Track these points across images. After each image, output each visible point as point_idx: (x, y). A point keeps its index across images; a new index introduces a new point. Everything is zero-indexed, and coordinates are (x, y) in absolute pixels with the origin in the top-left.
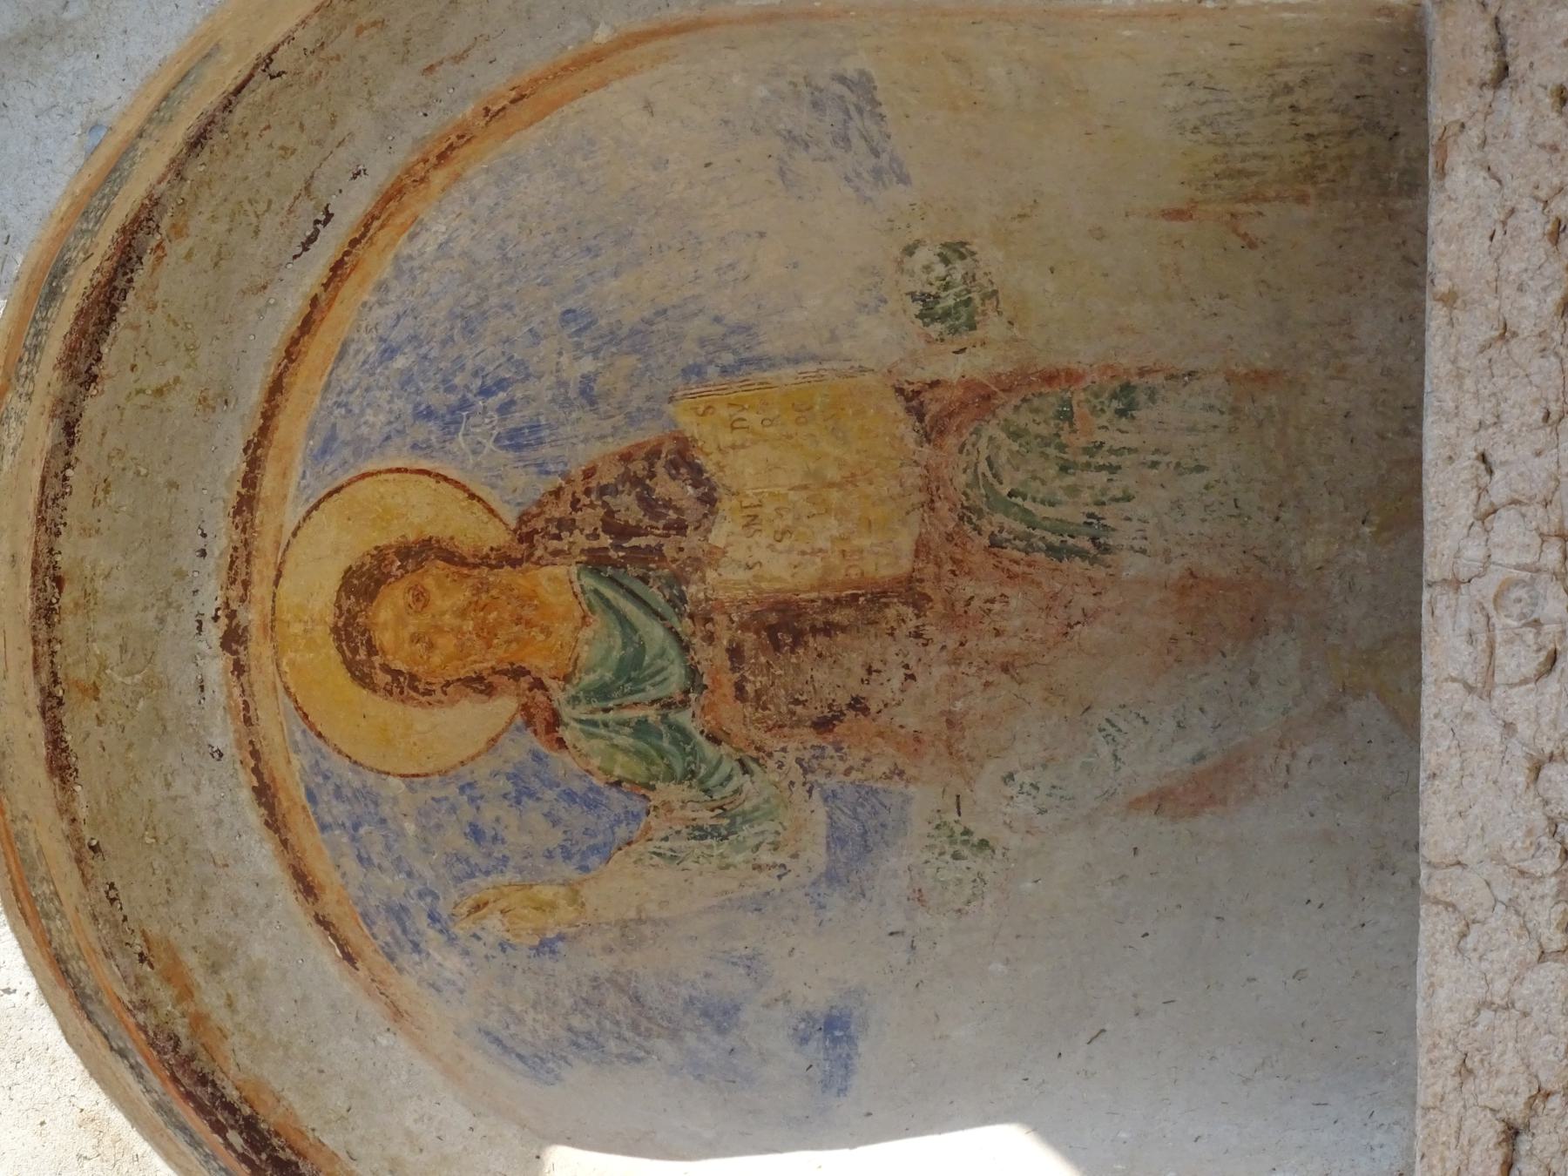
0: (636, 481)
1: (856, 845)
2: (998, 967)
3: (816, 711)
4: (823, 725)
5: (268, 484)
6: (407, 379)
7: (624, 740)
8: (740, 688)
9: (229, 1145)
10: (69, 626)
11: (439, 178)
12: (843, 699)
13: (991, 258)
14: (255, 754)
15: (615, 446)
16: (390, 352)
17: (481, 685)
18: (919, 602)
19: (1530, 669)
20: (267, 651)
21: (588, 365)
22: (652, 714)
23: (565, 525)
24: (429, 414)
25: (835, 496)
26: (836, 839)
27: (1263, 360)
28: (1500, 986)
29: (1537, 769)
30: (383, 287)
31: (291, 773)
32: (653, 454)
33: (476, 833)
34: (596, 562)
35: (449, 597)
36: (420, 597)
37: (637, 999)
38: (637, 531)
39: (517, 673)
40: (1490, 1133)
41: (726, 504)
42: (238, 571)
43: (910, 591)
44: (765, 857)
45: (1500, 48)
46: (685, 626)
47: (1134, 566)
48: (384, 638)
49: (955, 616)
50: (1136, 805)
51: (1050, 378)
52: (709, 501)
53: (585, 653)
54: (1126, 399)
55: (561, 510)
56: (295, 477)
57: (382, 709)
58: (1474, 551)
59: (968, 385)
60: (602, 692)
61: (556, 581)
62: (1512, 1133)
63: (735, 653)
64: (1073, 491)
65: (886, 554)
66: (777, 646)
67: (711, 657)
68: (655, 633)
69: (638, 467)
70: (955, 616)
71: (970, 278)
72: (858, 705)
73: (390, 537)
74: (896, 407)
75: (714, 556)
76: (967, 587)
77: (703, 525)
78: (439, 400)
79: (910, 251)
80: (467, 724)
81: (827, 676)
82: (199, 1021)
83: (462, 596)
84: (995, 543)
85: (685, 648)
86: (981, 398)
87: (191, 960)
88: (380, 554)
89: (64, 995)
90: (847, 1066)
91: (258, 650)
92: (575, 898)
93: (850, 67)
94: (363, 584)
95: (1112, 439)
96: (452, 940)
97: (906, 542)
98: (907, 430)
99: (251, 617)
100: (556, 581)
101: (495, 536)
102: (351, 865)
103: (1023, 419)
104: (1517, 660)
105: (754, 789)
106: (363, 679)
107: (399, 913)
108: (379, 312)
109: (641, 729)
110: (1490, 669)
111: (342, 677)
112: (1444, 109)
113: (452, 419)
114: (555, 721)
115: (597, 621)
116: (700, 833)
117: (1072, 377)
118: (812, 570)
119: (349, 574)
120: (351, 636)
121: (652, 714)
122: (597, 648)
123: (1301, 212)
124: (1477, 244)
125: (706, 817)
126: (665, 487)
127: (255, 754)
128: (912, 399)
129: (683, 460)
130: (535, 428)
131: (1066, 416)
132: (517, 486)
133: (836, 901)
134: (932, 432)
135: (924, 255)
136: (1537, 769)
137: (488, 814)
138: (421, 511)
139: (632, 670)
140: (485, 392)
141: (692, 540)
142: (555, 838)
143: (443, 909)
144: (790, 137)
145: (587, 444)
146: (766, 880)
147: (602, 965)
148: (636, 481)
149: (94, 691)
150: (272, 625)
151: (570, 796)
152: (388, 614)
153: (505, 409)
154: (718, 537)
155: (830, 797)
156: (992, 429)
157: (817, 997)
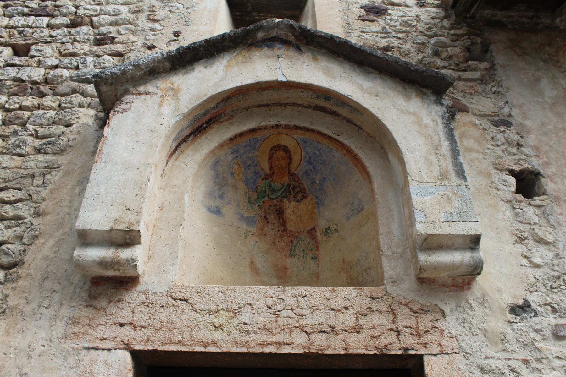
0: (301, 191)
1: (248, 220)
2: (227, 236)
3: (267, 216)
4: (265, 217)
5: (299, 132)
6: (315, 154)
7: (263, 189)
8: (271, 206)
9: (204, 123)
10: (279, 107)
11: (345, 152)
12: (269, 220)
13: (335, 236)
14: (260, 129)
15: (306, 187)
16: (319, 150)
17: (271, 168)
18: (283, 231)
19: (268, 303)
20: (275, 132)
21: (318, 182)
22: (267, 193)
23: (294, 181)
24: (310, 158)
25: (299, 219)
26: (248, 217)
27: (321, 277)
28: (212, 298)
29: (250, 305)
30: (328, 147)
31: (258, 136)
32: (305, 193)
33: (250, 166)
34: (289, 185)
35: (283, 163)
36: (284, 159)
37: (224, 186)
38: (294, 191)
39: (273, 174)
40: (186, 297)
41: (298, 204)
42: (287, 127)
43: (285, 230)
44: (246, 208)
45: (378, 298)
46: (280, 198)
47: (289, 261)
48: (278, 153)
49: (281, 236)
50: (252, 259)
51: (317, 247)
52: (298, 201)
53: (276, 184)
54: (315, 258)
55: (296, 180)
56: (301, 137)
57: (268, 151)
58: (289, 295)
59: (316, 236)
60: (270, 186)
61: (286, 180)
62: (186, 300)
63: (276, 205)
64: (300, 252)
65: (291, 227)
66: (277, 211)
67: (275, 202)
68: (279, 194)
69: (303, 191)
70: (281, 236)
71: (332, 233)
72: (268, 222)
73: (292, 154)
74: (312, 227)
75: (290, 202)
76: (285, 237)
77: (295, 201)
78: (312, 159)
79: (336, 225)
80: (265, 166)
81: (271, 218)
82: (222, 122)
83: (284, 165)
84: (292, 241)
85: (277, 198)
86: (314, 238)
87: (231, 121)
88: (290, 152)
89: (225, 96)
90: (212, 212)
91: (275, 131)
92: (240, 179)
93: (366, 207)
94: (285, 149)
95: (308, 257)
96: (234, 159)
97: (292, 229)
98: (309, 228)
99: (280, 129)
100: (286, 180)
101: (293, 170)
102: (244, 144)
103: (311, 244)
104: (270, 302)
105: (256, 207)
106: (272, 149)
107: (237, 151)
108: (324, 147)
109: (265, 192)
110: (268, 297)
111: (272, 146)
112: (366, 289)
113: (309, 162)
114: (266, 179)
115: (281, 186)
116: (249, 199)
117: (318, 250)
118: (288, 216)
119: (286, 147)
120: (278, 147)
121: (267, 193)
122: (277, 186)
123: (345, 280)
124: (343, 295)
125: (252, 200)
126: (300, 195)
127: (260, 129)
128: (314, 229)
129: (304, 197)
130: (308, 175)
131: (312, 250)
132: (300, 173)
133: (239, 216)
134: (309, 232)
135: (335, 227)
136: (250, 305)
137: (253, 168)
138: (296, 158)
139: (273, 191)
140: (313, 167)
141: (292, 199)
142: (249, 178)
143: (238, 159)
144: (353, 203)
145: (306, 183)
146: (242, 207)
147: (230, 182)
148: (301, 191)
149: (270, 110)
150: (279, 133)
151: (255, 180)
152: (281, 153)
153: (311, 170)
154: (293, 203)
155: (254, 217)
156: (309, 240)
157: (224, 211)
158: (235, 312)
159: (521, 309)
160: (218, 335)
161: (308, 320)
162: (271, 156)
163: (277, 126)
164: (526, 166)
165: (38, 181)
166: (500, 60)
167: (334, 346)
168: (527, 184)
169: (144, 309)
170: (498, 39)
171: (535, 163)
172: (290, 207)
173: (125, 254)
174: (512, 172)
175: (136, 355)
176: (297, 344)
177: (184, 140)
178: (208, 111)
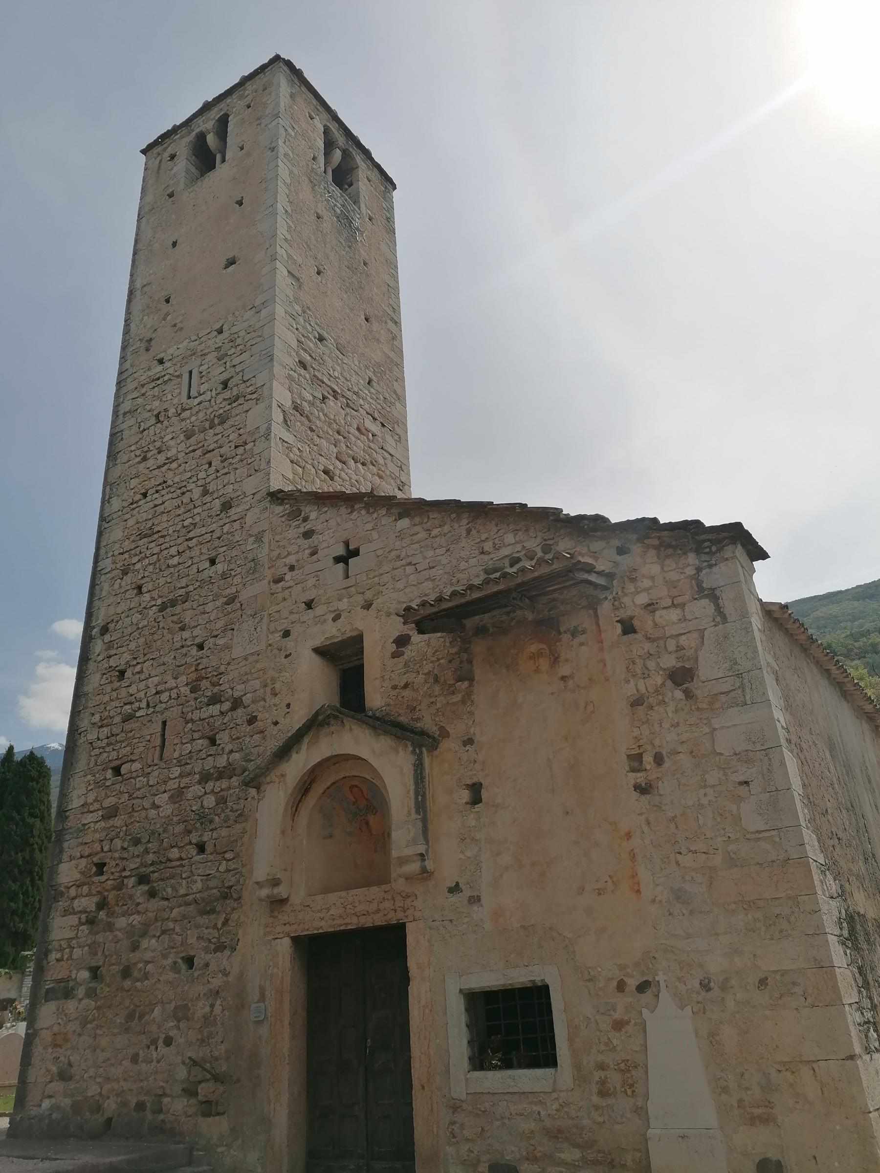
42: (349, 777)
43: (371, 834)
94: (356, 786)
152: (355, 789)
158: (328, 909)
159: (455, 889)
160: (323, 923)
161: (357, 909)
162: (351, 792)
163: (344, 778)
164: (475, 780)
165: (239, 844)
166: (478, 673)
167: (367, 922)
168: (476, 792)
169: (293, 914)
170: (479, 647)
171: (480, 777)
172: (371, 818)
173: (276, 891)
174: (468, 786)
175: (294, 939)
176: (353, 923)
177: (300, 801)
178: (305, 782)
